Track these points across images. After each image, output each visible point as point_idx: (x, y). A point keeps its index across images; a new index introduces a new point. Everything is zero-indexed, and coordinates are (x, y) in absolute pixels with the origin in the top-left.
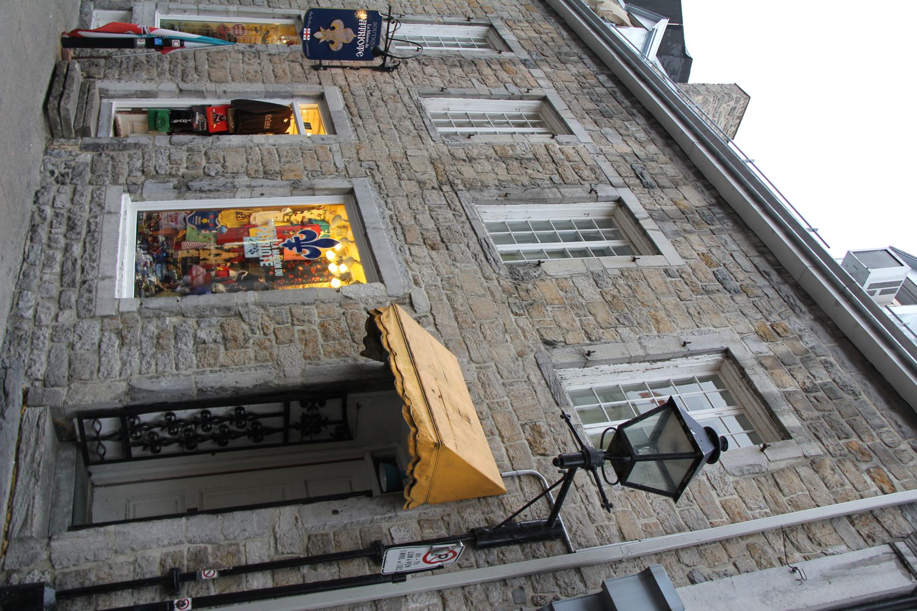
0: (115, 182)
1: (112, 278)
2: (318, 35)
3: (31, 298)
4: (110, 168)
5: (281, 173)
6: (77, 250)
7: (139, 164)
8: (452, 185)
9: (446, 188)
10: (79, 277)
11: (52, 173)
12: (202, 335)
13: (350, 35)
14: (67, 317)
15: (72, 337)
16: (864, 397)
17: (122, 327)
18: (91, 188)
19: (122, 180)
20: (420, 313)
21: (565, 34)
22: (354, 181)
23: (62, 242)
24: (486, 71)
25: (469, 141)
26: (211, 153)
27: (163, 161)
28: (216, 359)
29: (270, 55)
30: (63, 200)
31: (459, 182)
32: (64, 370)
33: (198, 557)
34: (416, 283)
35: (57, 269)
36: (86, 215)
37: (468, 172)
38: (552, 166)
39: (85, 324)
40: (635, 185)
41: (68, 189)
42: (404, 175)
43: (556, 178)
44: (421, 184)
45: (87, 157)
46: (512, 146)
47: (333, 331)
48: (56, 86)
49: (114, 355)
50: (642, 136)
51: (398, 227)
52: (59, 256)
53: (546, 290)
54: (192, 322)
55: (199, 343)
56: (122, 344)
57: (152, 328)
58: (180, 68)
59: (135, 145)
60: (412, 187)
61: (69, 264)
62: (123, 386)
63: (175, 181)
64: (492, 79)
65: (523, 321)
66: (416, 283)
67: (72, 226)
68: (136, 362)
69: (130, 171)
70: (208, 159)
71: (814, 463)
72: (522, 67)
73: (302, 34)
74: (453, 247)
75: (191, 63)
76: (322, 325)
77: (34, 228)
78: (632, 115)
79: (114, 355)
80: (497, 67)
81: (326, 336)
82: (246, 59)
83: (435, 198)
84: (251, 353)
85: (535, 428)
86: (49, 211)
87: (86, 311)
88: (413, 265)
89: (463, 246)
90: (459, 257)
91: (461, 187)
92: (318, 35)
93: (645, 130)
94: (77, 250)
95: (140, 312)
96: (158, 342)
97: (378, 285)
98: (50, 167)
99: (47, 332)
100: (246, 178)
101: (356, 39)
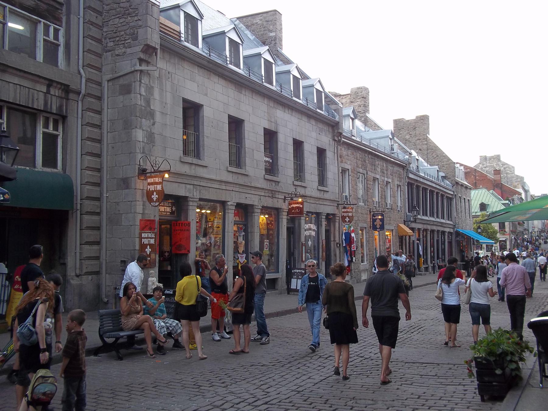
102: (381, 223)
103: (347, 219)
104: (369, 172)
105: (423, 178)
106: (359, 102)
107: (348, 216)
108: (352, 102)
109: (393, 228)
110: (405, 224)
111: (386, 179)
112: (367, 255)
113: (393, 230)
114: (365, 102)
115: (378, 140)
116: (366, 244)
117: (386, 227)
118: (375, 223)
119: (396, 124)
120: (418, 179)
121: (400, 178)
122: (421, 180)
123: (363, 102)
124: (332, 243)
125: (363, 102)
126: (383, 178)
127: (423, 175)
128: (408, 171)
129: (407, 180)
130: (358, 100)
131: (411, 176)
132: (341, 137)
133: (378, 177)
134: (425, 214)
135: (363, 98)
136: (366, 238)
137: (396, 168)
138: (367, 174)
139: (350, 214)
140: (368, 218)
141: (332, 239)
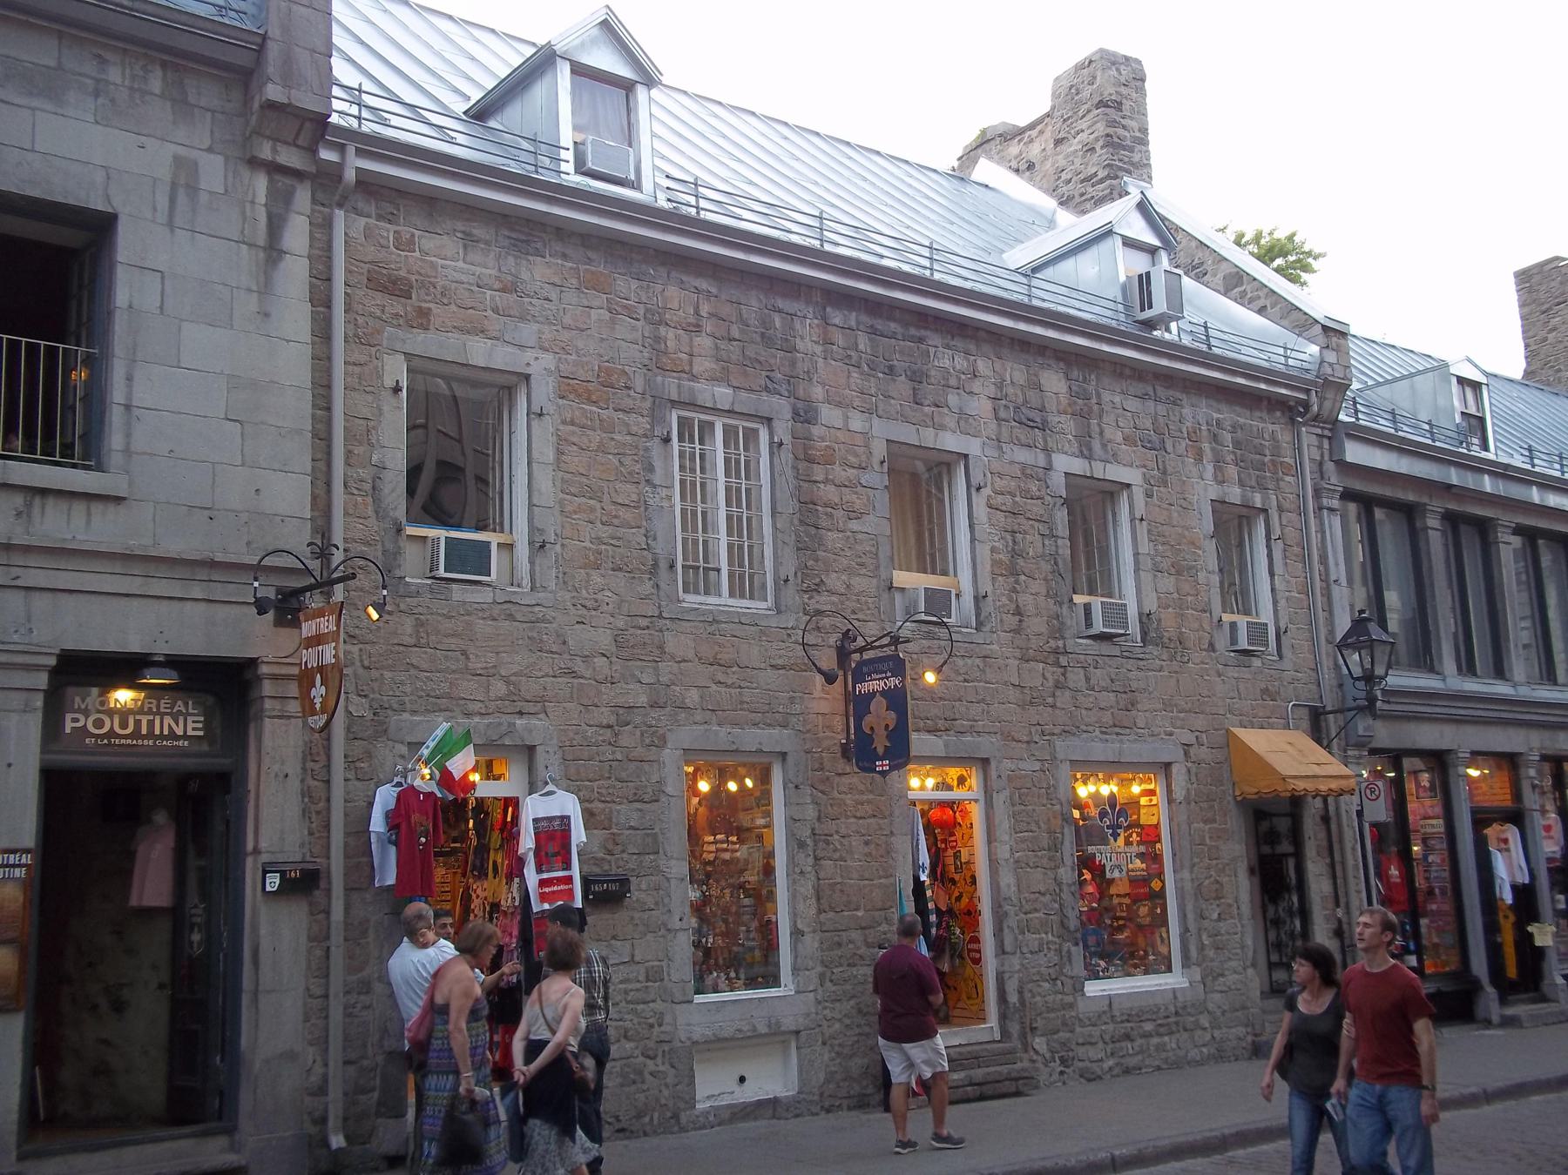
0: (1071, 1006)
1: (1174, 991)
2: (880, 750)
3: (1194, 1054)
4: (1052, 1015)
5: (1051, 832)
6: (1148, 1027)
7: (1046, 985)
8: (1056, 652)
9: (1063, 660)
10: (1172, 1020)
11: (1062, 1073)
12: (1215, 916)
13: (878, 705)
14: (1204, 1021)
15: (1219, 1013)
16: (1242, 420)
17: (1210, 977)
18: (1078, 1029)
19: (1070, 999)
20: (1193, 741)
21: (703, 284)
22: (1060, 756)
23: (1139, 1041)
24: (829, 493)
25: (990, 599)
26: (1027, 907)
27: (1042, 960)
28: (1230, 906)
29: (819, 819)
30: (1093, 1053)
31: (1052, 643)
32: (1239, 1014)
33: (1327, 918)
34: (1171, 734)
35: (1166, 1039)
36: (1111, 1027)
37: (1036, 625)
38: (1021, 520)
39: (1211, 1006)
40: (1046, 441)
41: (1081, 1051)
42: (1050, 700)
43: (1043, 529)
44: (1058, 686)
45: (1039, 1043)
46: (993, 550)
47: (1209, 815)
48: (1005, 1090)
49: (1231, 978)
50: (960, 362)
51: (1117, 730)
52: (1155, 1040)
53: (1168, 620)
54: (1206, 923)
55: (1220, 918)
56: (1222, 975)
57: (1211, 953)
58: (863, 951)
59: (1020, 992)
60: (1064, 698)
61: (1162, 1030)
62: (1250, 971)
63: (1066, 946)
64: (848, 495)
65: (1197, 656)
66: (1171, 734)
67: (1128, 1037)
68: (1233, 964)
69: (1057, 993)
70: (1036, 910)
71: (1280, 509)
72: (816, 431)
73: (884, 774)
74: (1134, 685)
75: (856, 935)
76: (1205, 822)
77: (1127, 1071)
78: (921, 340)
79: (1231, 978)
80: (818, 473)
81: (1214, 821)
82: (836, 856)
83: (1076, 678)
84: (1226, 879)
85: (1265, 691)
86: (1111, 1062)
87: (1202, 1008)
88: (1157, 730)
89: (1130, 675)
90: (1142, 685)
91: (1060, 643)
92: (880, 750)
93: (948, 347)
94: (1148, 1027)
95: (1199, 965)
96: (1218, 948)
97: (1175, 769)
98: (1056, 1076)
99: (1217, 1034)
100: (1061, 871)
101: (883, 693)
102: (891, 717)
103: (318, 691)
104: (829, 415)
105: (1503, 472)
106: (1091, 128)
107: (321, 669)
108: (1058, 142)
109: (1170, 752)
110: (1317, 733)
111: (1067, 463)
112: (797, 933)
113: (1167, 766)
114: (1112, 123)
115: (1068, 265)
116: (791, 859)
117: (920, 742)
118: (868, 721)
119: (1530, 290)
120: (1454, 477)
121: (1255, 462)
122: (1487, 484)
123: (1101, 128)
124: (249, 861)
125: (1101, 128)
126: (1023, 456)
127: (1518, 461)
128: (1335, 433)
129: (1334, 479)
130: (1083, 124)
131: (1356, 453)
132: (341, 149)
133: (951, 442)
134: (1424, 658)
135: (1102, 104)
136: (792, 821)
137: (1197, 413)
138: (804, 415)
139: (328, 653)
140: (824, 701)
141: (250, 846)
